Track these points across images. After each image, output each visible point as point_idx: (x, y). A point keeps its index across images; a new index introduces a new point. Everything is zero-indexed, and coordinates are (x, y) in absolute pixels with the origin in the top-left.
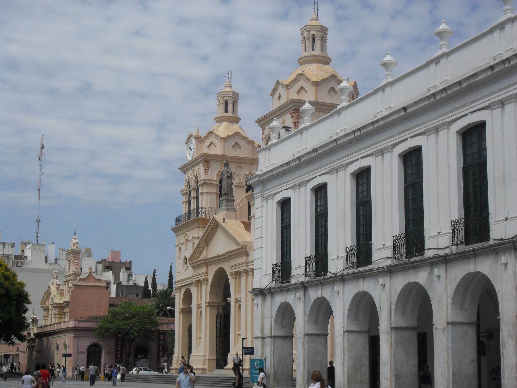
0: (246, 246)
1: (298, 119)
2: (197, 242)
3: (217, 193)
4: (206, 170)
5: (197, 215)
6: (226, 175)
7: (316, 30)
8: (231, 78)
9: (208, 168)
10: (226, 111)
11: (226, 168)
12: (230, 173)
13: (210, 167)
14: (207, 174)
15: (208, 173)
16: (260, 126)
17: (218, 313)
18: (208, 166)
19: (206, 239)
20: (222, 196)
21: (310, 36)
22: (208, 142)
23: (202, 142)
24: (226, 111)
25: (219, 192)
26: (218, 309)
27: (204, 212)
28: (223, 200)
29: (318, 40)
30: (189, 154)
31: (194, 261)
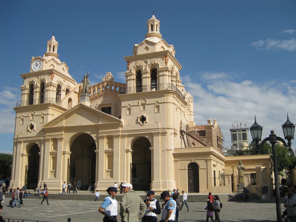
14: (52, 80)
16: (126, 60)
22: (50, 64)
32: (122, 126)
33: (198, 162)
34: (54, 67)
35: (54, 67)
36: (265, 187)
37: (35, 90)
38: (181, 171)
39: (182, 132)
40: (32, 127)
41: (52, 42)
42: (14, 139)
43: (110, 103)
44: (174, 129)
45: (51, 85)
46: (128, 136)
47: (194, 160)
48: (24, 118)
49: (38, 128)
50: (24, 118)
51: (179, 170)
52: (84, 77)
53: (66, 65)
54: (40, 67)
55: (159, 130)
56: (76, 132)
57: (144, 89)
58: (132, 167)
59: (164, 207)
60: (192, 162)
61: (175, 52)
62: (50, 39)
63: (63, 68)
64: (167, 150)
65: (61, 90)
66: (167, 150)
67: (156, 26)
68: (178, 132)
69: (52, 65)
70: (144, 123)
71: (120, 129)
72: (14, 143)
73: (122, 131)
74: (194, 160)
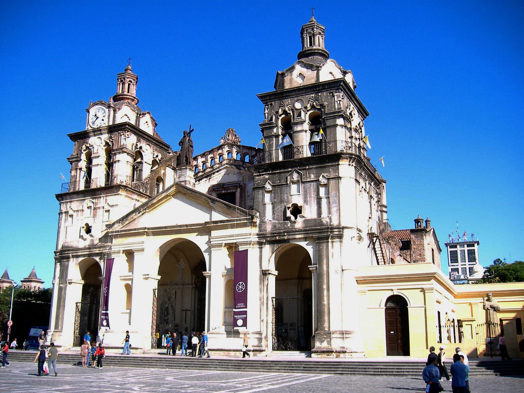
33: (406, 294)
34: (129, 119)
35: (129, 119)
37: (95, 162)
39: (371, 235)
40: (88, 230)
42: (55, 253)
45: (122, 150)
48: (75, 214)
49: (98, 232)
50: (75, 214)
52: (184, 134)
54: (103, 120)
57: (296, 153)
63: (147, 122)
65: (144, 161)
68: (364, 235)
70: (298, 217)
72: (56, 259)
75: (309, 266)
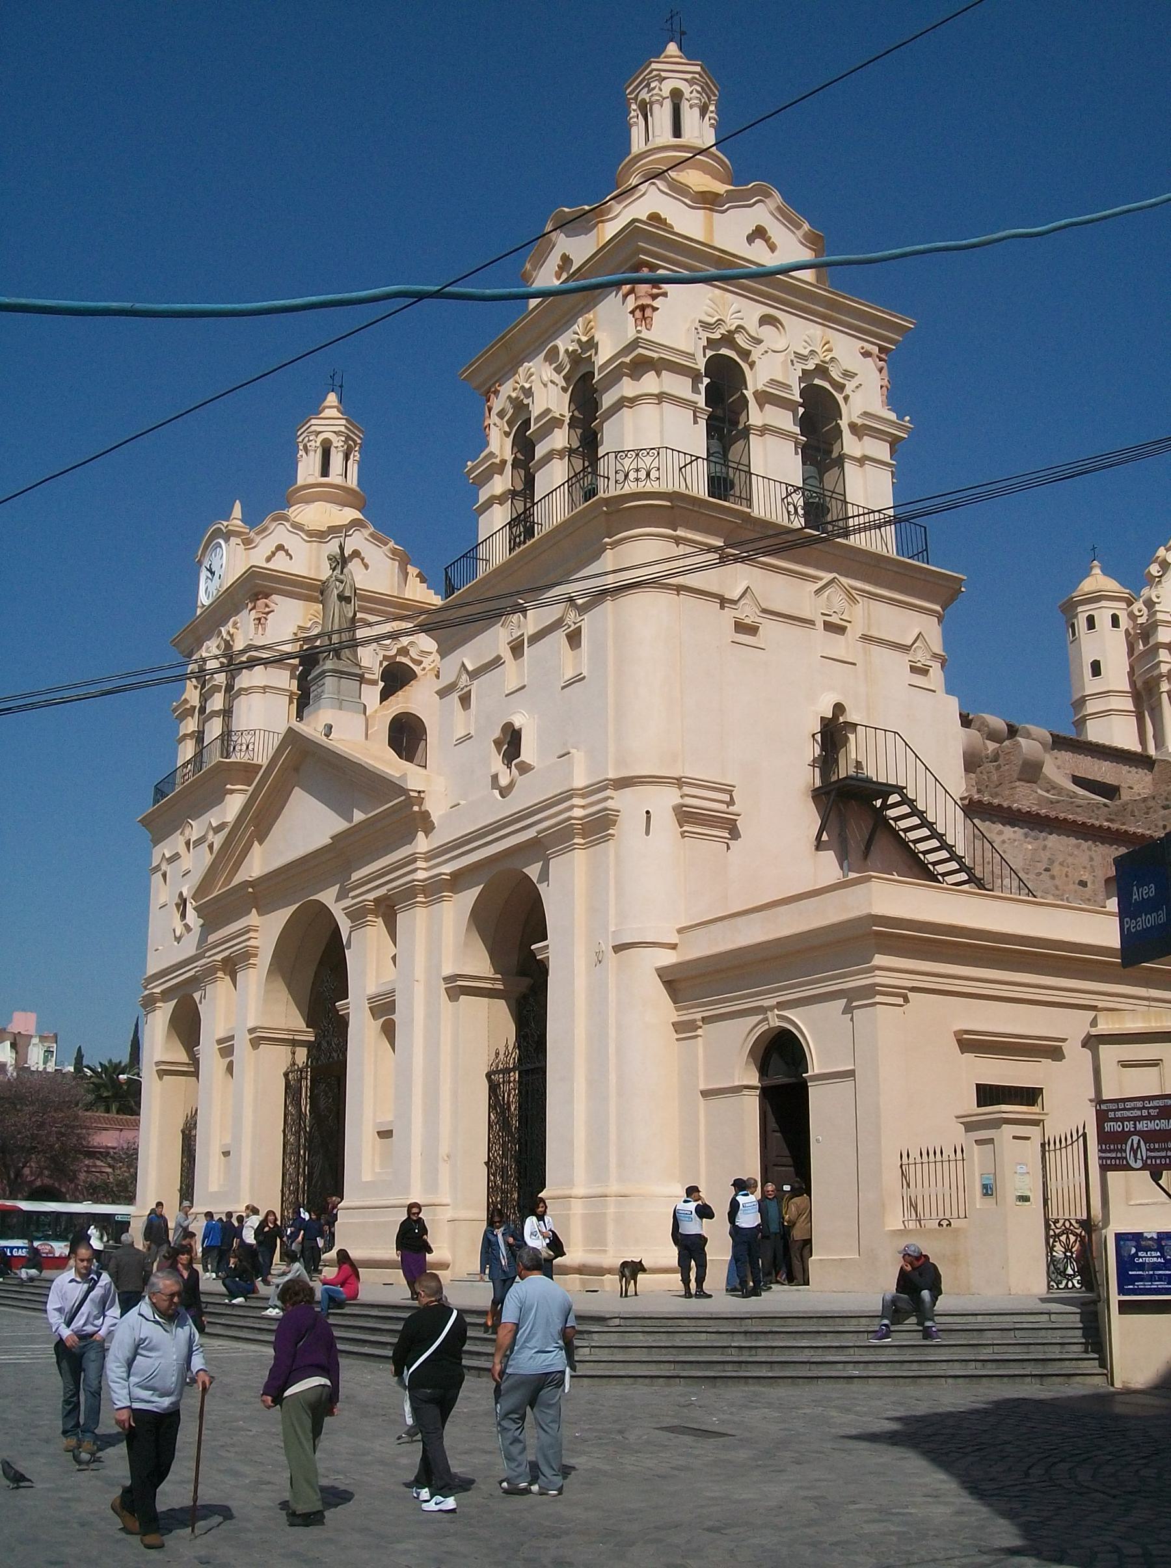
0: (422, 795)
1: (654, 297)
2: (218, 840)
3: (292, 694)
4: (259, 619)
5: (226, 753)
6: (336, 592)
7: (686, 80)
8: (341, 386)
9: (268, 613)
10: (325, 472)
11: (338, 571)
12: (351, 586)
13: (272, 611)
15: (264, 629)
17: (294, 1064)
18: (267, 610)
19: (257, 816)
20: (321, 663)
21: (666, 92)
23: (250, 545)
24: (325, 472)
25: (298, 690)
26: (294, 1053)
27: (251, 747)
28: (324, 672)
29: (691, 107)
30: (207, 588)
31: (212, 894)
32: (425, 823)
36: (1138, 1237)
38: (717, 1102)
41: (313, 428)
43: (520, 686)
44: (679, 782)
46: (457, 882)
47: (780, 1006)
51: (705, 1094)
53: (372, 529)
55: (572, 807)
56: (298, 903)
58: (309, 1094)
59: (479, 1396)
60: (772, 1024)
61: (806, 227)
62: (315, 409)
64: (618, 948)
66: (618, 948)
67: (668, 104)
69: (280, 548)
71: (422, 844)
73: (430, 856)
74: (780, 1006)
75: (533, 947)
